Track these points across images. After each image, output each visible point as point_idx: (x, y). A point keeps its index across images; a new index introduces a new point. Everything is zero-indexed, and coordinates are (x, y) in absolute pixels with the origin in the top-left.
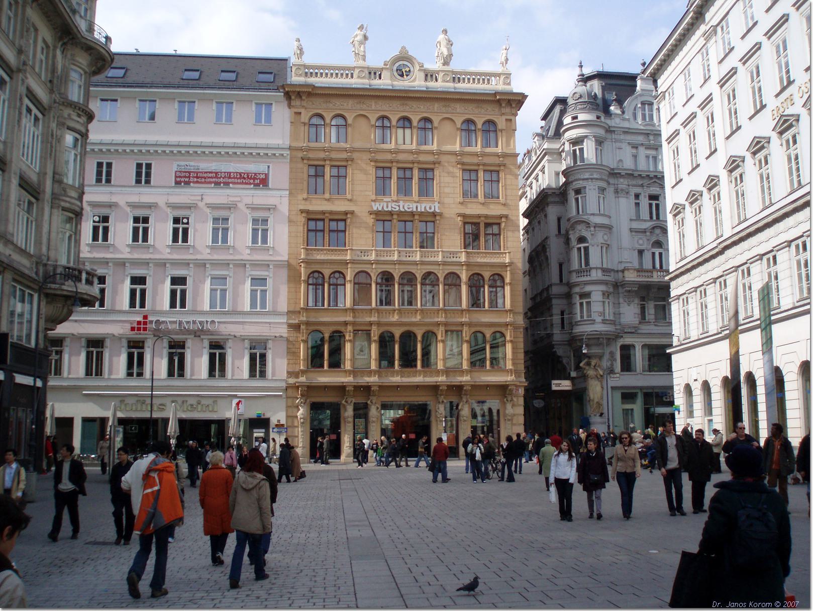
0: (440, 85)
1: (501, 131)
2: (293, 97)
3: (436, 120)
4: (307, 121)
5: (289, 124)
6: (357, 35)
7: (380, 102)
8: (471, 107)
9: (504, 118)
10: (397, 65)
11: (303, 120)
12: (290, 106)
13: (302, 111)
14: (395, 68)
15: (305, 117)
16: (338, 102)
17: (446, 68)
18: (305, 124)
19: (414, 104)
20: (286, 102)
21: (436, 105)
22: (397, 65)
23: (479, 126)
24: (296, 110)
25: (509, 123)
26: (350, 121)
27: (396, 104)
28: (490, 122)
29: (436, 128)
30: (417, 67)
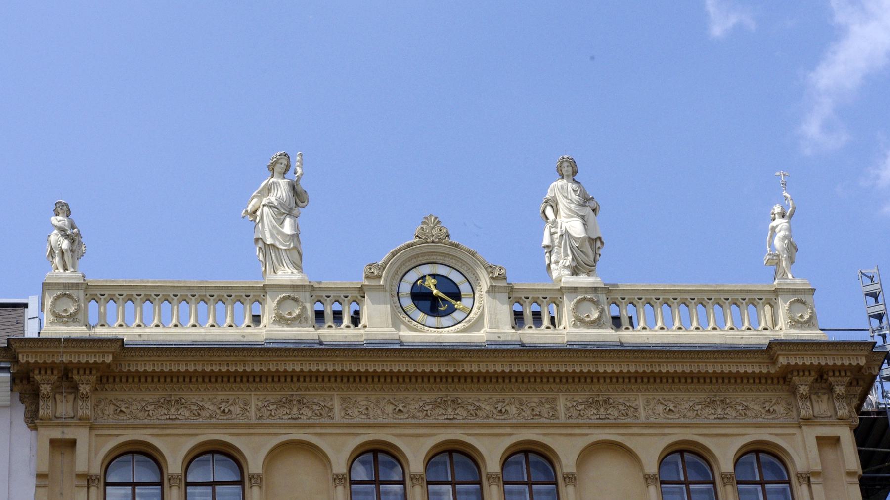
0: (567, 331)
1: (807, 478)
2: (45, 389)
3: (567, 451)
4: (96, 469)
5: (33, 481)
6: (269, 189)
7: (362, 397)
8: (687, 400)
9: (811, 434)
10: (412, 277)
11: (81, 466)
12: (33, 420)
13: (81, 435)
14: (406, 288)
15: (89, 455)
16: (209, 400)
17: (583, 280)
18: (89, 480)
19: (485, 400)
20: (20, 411)
21: (562, 402)
22: (412, 277)
23: (726, 464)
24: (57, 434)
25: (830, 453)
26: (255, 465)
27: (417, 400)
28: (757, 451)
29: (570, 478)
30: (485, 282)
